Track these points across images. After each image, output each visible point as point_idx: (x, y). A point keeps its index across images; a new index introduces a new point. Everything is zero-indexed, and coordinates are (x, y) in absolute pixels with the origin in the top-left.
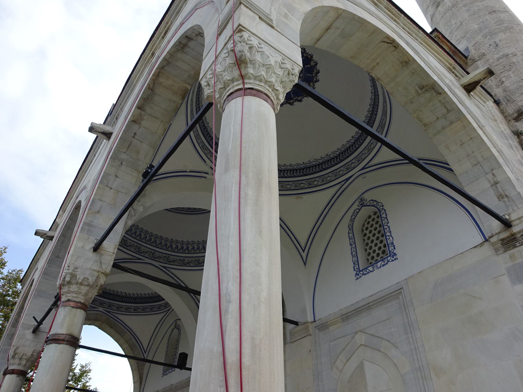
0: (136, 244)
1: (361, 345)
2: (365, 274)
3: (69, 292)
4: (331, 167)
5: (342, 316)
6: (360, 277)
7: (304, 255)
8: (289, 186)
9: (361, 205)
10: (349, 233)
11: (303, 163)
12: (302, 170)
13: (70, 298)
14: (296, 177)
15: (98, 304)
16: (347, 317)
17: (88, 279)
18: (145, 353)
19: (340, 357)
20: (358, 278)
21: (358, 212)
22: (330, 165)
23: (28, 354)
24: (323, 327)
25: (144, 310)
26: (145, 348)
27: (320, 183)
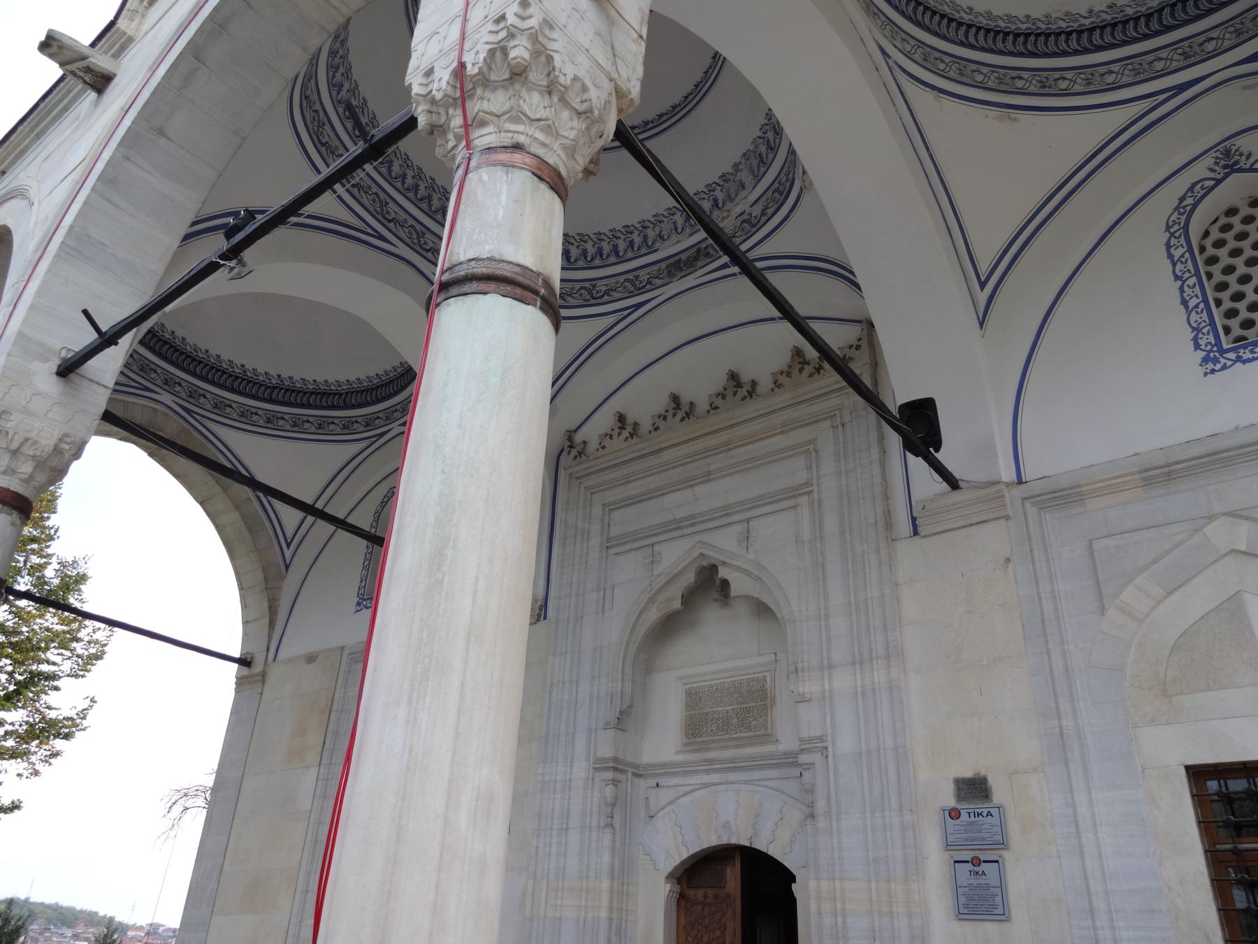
0: (375, 189)
1: (1233, 551)
2: (1249, 360)
3: (518, 116)
4: (1125, 43)
5: (1146, 470)
6: (1225, 367)
7: (982, 297)
8: (979, 78)
9: (1225, 167)
10: (1168, 246)
11: (1028, 17)
12: (1021, 39)
13: (522, 139)
14: (1001, 53)
16: (1169, 473)
17: (584, 89)
18: (288, 545)
19: (1137, 581)
20: (1213, 371)
21: (1212, 188)
22: (1119, 36)
23: (43, 442)
24: (1063, 497)
25: (296, 424)
27: (1077, 88)
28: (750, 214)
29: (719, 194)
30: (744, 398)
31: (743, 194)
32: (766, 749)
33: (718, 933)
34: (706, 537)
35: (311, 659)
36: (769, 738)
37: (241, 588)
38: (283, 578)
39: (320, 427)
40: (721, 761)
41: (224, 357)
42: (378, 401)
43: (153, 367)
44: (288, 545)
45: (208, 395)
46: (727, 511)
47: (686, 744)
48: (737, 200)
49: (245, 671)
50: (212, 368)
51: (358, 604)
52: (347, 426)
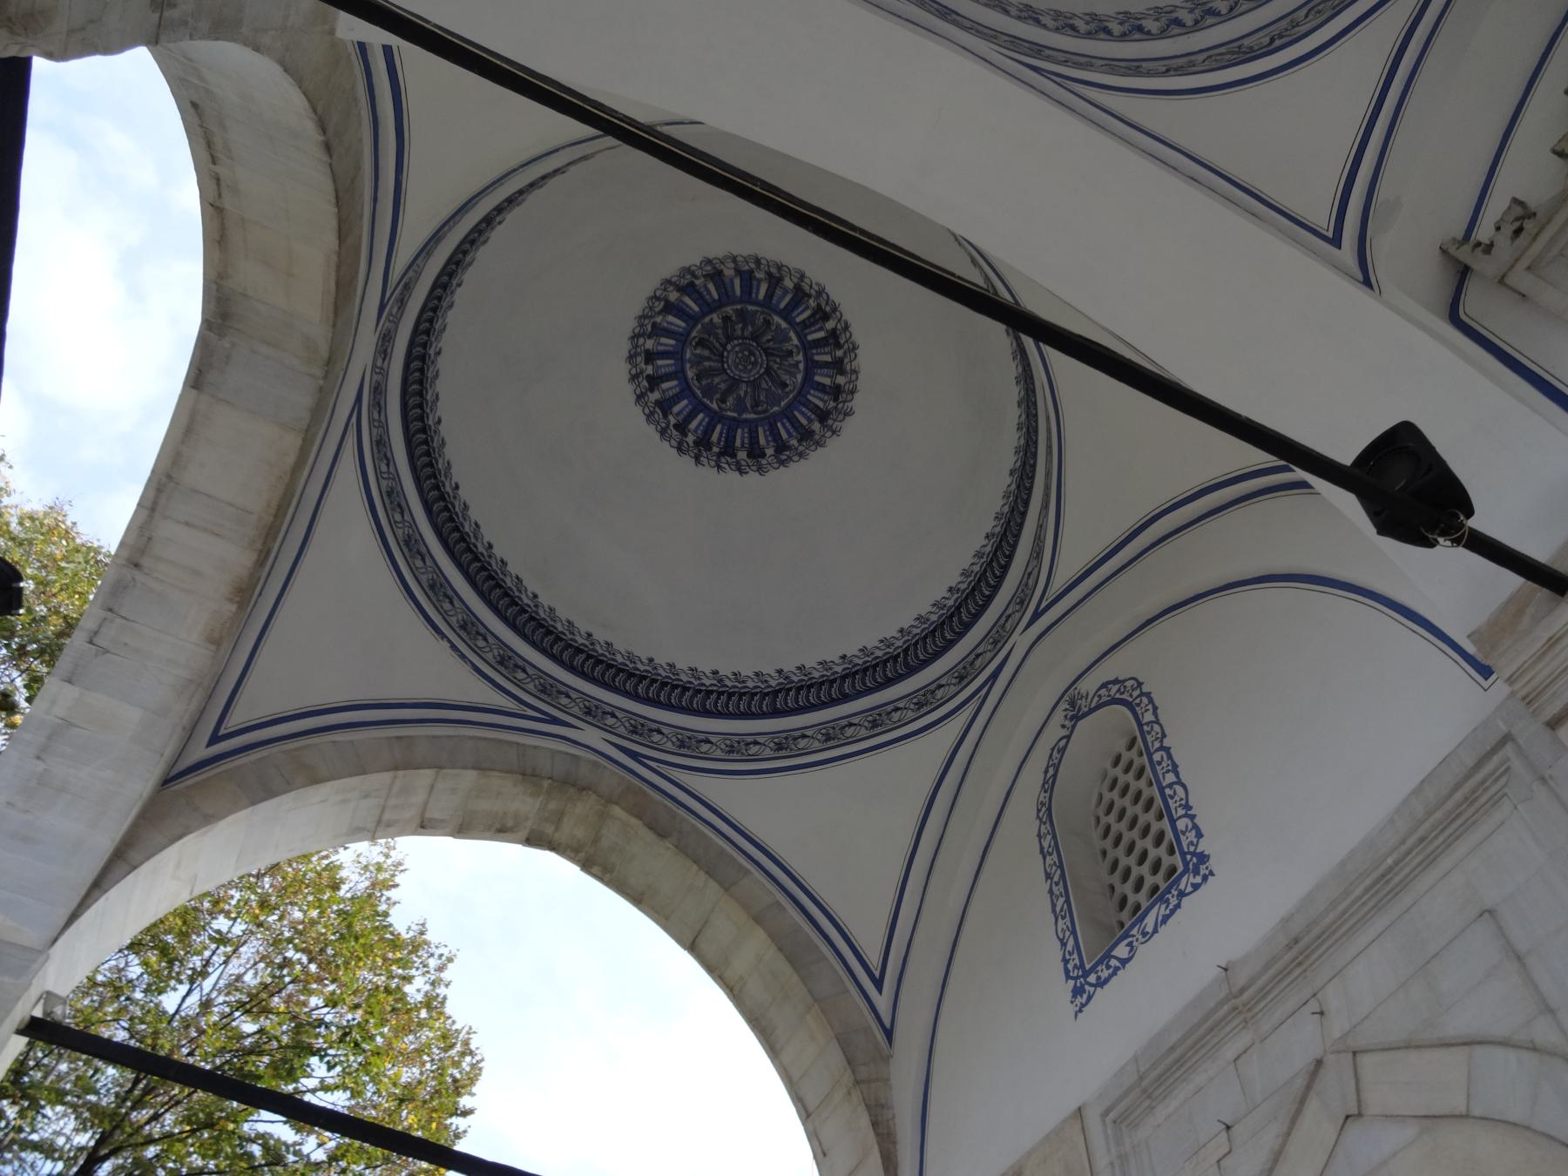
15: (576, 710)
25: (830, 735)
26: (874, 960)
37: (806, 1114)
38: (887, 1059)
39: (874, 724)
41: (682, 665)
43: (563, 689)
44: (879, 984)
45: (665, 730)
50: (664, 684)
51: (1077, 991)
52: (924, 700)
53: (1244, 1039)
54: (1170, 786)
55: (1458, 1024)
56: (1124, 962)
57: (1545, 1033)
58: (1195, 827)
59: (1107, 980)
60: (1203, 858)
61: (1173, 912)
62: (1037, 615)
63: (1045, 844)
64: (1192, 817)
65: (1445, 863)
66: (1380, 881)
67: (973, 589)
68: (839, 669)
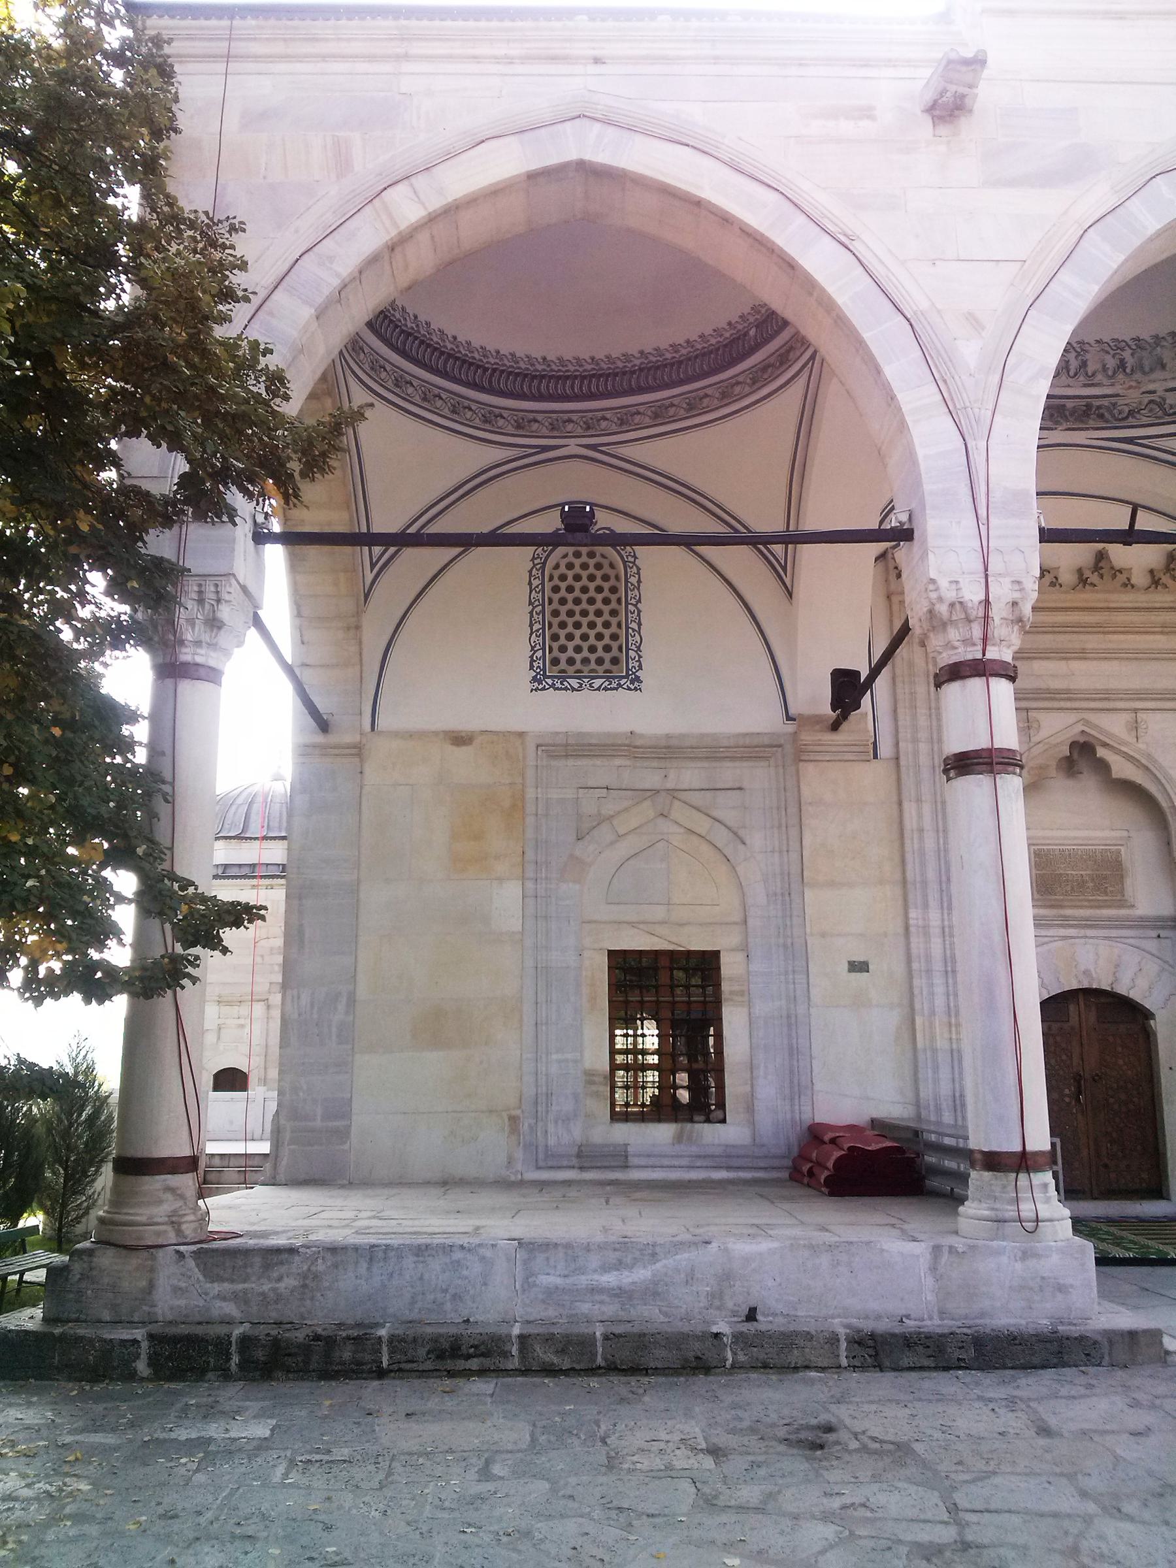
28: (1164, 400)
29: (1127, 354)
30: (1125, 585)
31: (1158, 374)
32: (1123, 912)
33: (1064, 1057)
34: (1092, 717)
35: (460, 739)
36: (1122, 903)
40: (1075, 918)
42: (541, 398)
44: (373, 566)
46: (1107, 695)
47: (1038, 900)
48: (1153, 376)
49: (320, 739)
51: (534, 679)
53: (628, 763)
54: (634, 630)
55: (715, 813)
56: (573, 689)
57: (742, 833)
58: (639, 661)
59: (558, 689)
60: (638, 679)
61: (611, 689)
62: (593, 447)
63: (535, 583)
64: (640, 657)
65: (737, 764)
66: (712, 751)
67: (559, 378)
68: (449, 346)
